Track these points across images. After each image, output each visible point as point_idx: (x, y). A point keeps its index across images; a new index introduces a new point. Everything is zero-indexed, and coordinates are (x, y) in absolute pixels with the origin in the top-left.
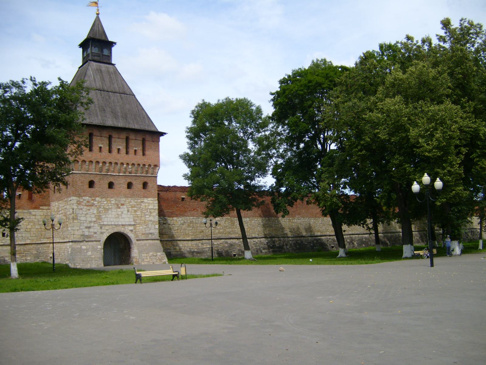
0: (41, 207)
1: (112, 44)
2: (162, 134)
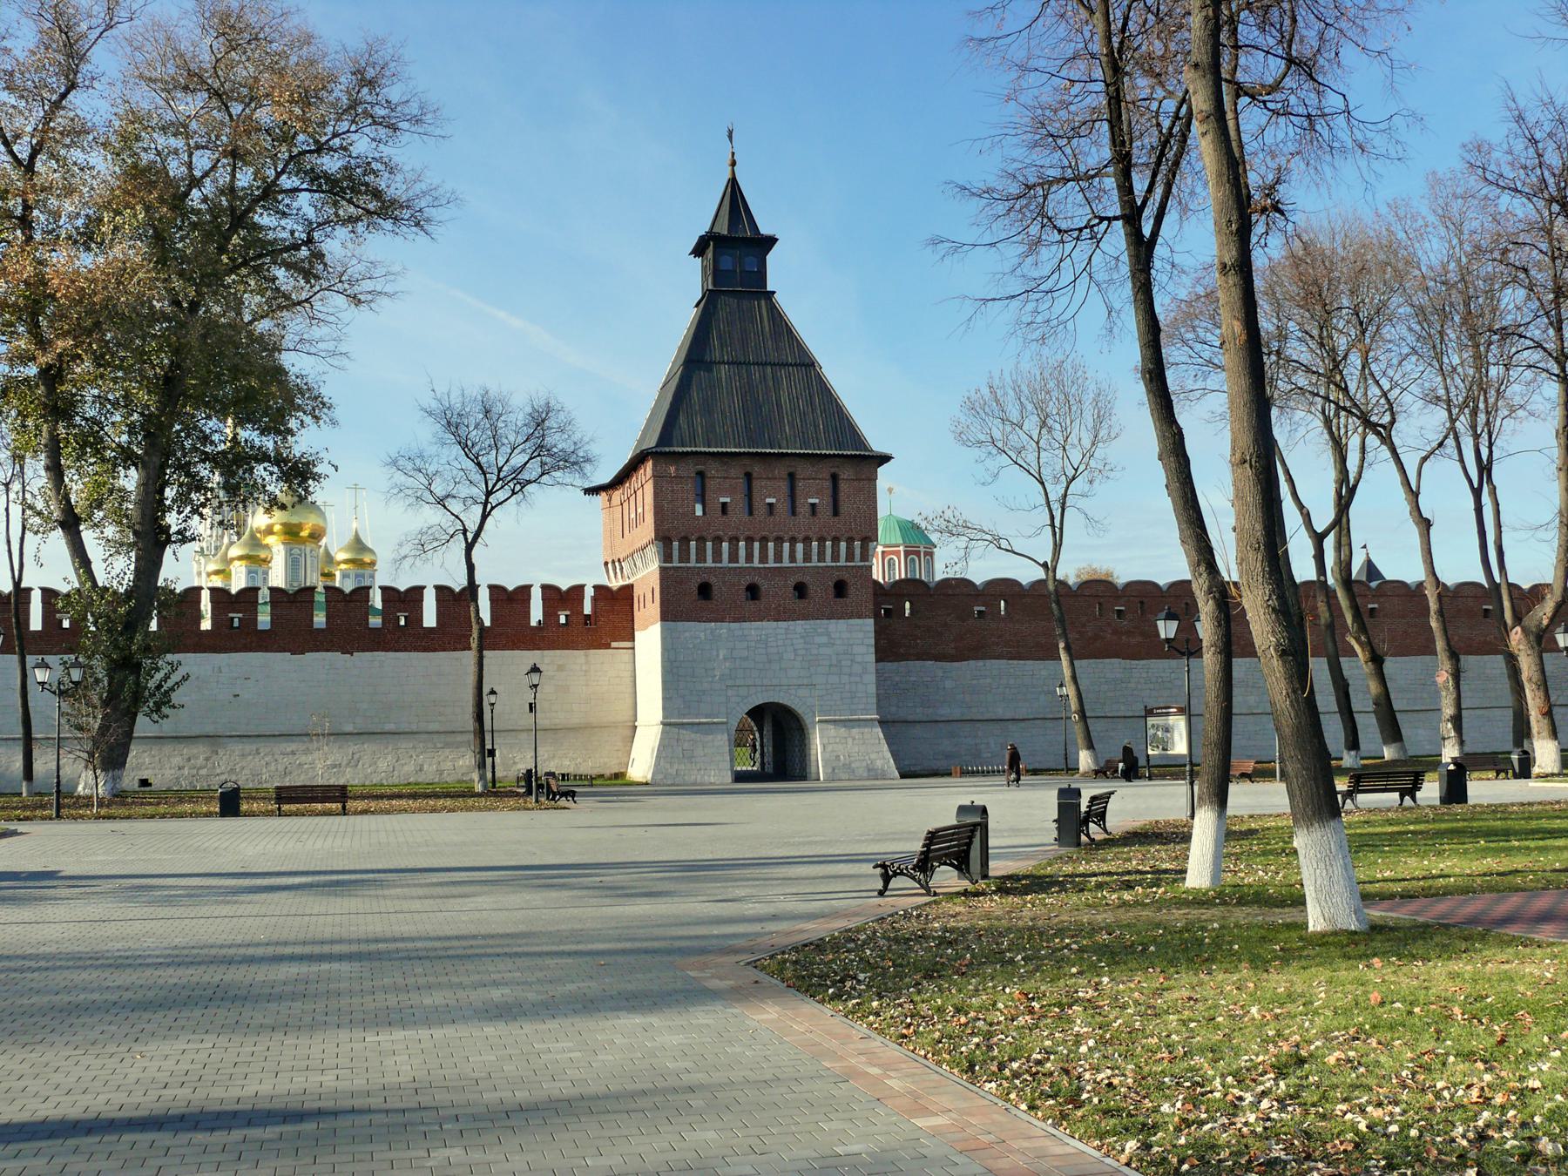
0: (614, 644)
1: (771, 241)
2: (885, 459)
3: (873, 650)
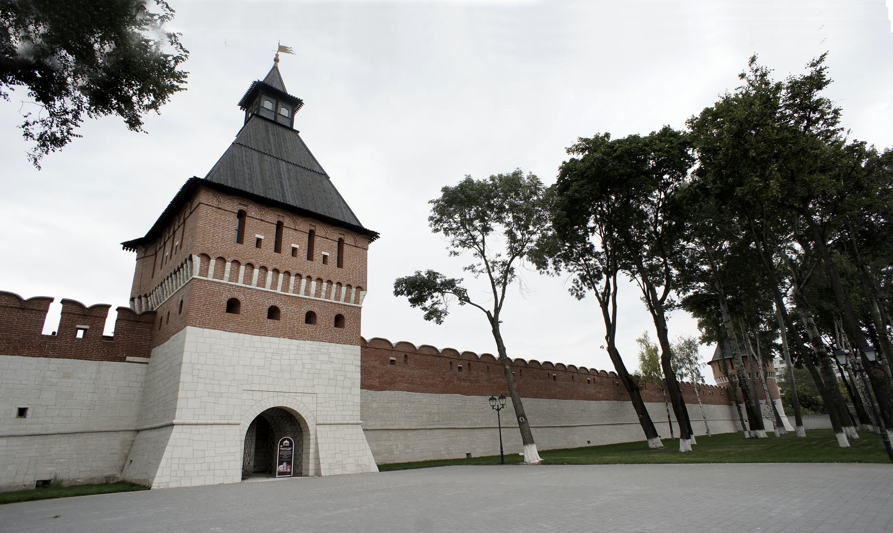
0: (128, 358)
3: (359, 369)
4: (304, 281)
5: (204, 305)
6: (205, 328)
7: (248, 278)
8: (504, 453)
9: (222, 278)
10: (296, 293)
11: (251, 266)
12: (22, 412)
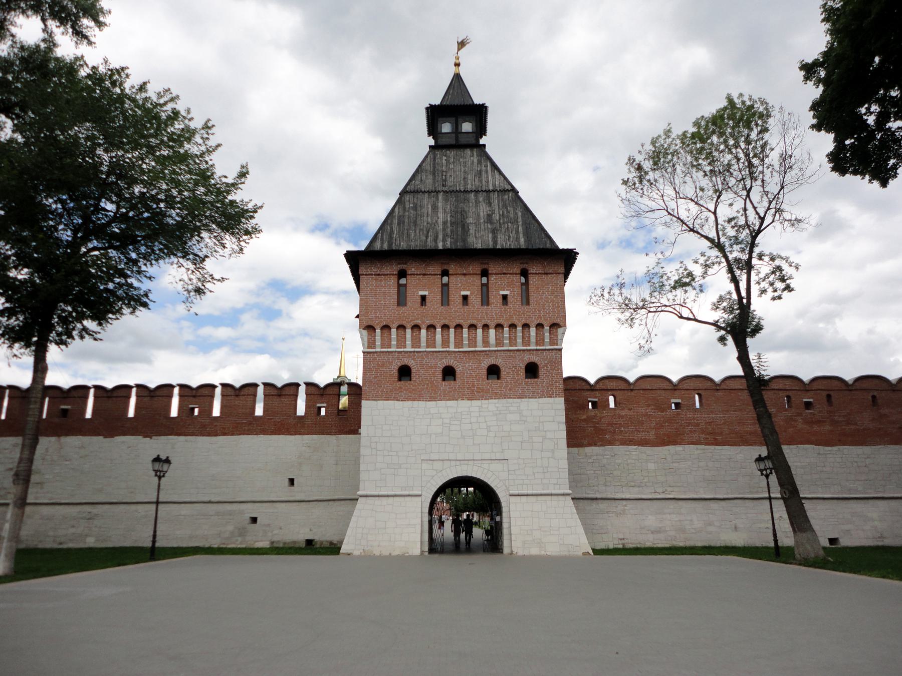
3: (564, 427)
4: (480, 331)
5: (375, 377)
6: (379, 400)
7: (416, 342)
8: (157, 545)
9: (390, 346)
10: (473, 347)
11: (416, 327)
12: (292, 482)
